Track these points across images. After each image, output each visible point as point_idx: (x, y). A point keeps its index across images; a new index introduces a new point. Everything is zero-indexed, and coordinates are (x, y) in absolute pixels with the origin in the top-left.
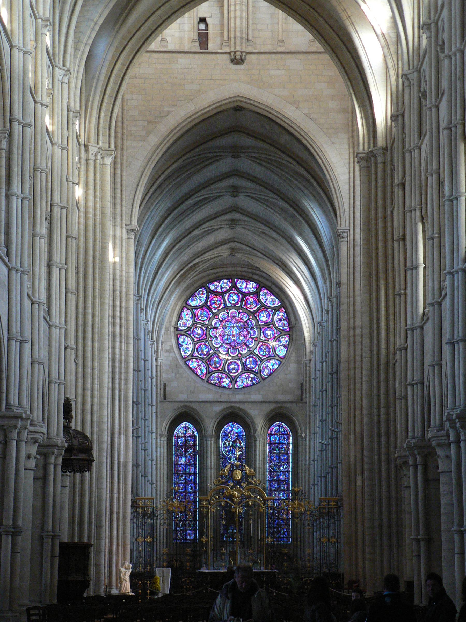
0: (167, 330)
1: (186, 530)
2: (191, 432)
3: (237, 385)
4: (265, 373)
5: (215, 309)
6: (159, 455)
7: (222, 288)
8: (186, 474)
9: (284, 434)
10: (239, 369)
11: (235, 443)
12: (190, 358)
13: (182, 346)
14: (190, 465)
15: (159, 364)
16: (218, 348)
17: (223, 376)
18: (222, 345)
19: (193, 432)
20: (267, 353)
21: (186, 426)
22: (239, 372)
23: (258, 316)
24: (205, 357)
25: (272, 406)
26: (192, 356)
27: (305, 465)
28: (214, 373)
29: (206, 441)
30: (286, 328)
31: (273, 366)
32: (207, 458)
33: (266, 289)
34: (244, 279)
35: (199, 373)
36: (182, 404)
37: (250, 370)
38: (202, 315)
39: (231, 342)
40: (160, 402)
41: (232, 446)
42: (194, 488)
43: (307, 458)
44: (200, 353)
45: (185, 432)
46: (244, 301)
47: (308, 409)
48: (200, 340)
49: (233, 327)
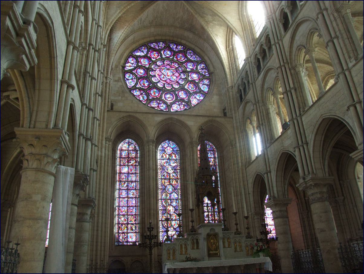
0: (117, 67)
1: (127, 233)
2: (133, 147)
3: (173, 109)
4: (194, 102)
5: (154, 58)
6: (103, 155)
7: (159, 46)
8: (128, 181)
9: (211, 150)
10: (173, 98)
11: (171, 156)
12: (133, 88)
13: (128, 80)
14: (132, 173)
15: (109, 82)
16: (157, 83)
17: (161, 102)
18: (159, 81)
19: (135, 147)
20: (194, 89)
21: (129, 142)
22: (174, 100)
23: (186, 65)
24: (146, 88)
25: (206, 119)
26: (136, 87)
27: (238, 167)
28: (154, 100)
29: (149, 146)
30: (207, 74)
31: (199, 98)
32: (149, 160)
33: (191, 50)
34: (175, 43)
35: (141, 99)
36: (127, 114)
37: (182, 100)
38: (144, 62)
39: (166, 80)
40: (108, 111)
41: (169, 159)
42: (135, 194)
43: (240, 161)
44: (142, 85)
45: (127, 146)
46: (175, 55)
47: (235, 122)
48: (142, 77)
49: (168, 69)
